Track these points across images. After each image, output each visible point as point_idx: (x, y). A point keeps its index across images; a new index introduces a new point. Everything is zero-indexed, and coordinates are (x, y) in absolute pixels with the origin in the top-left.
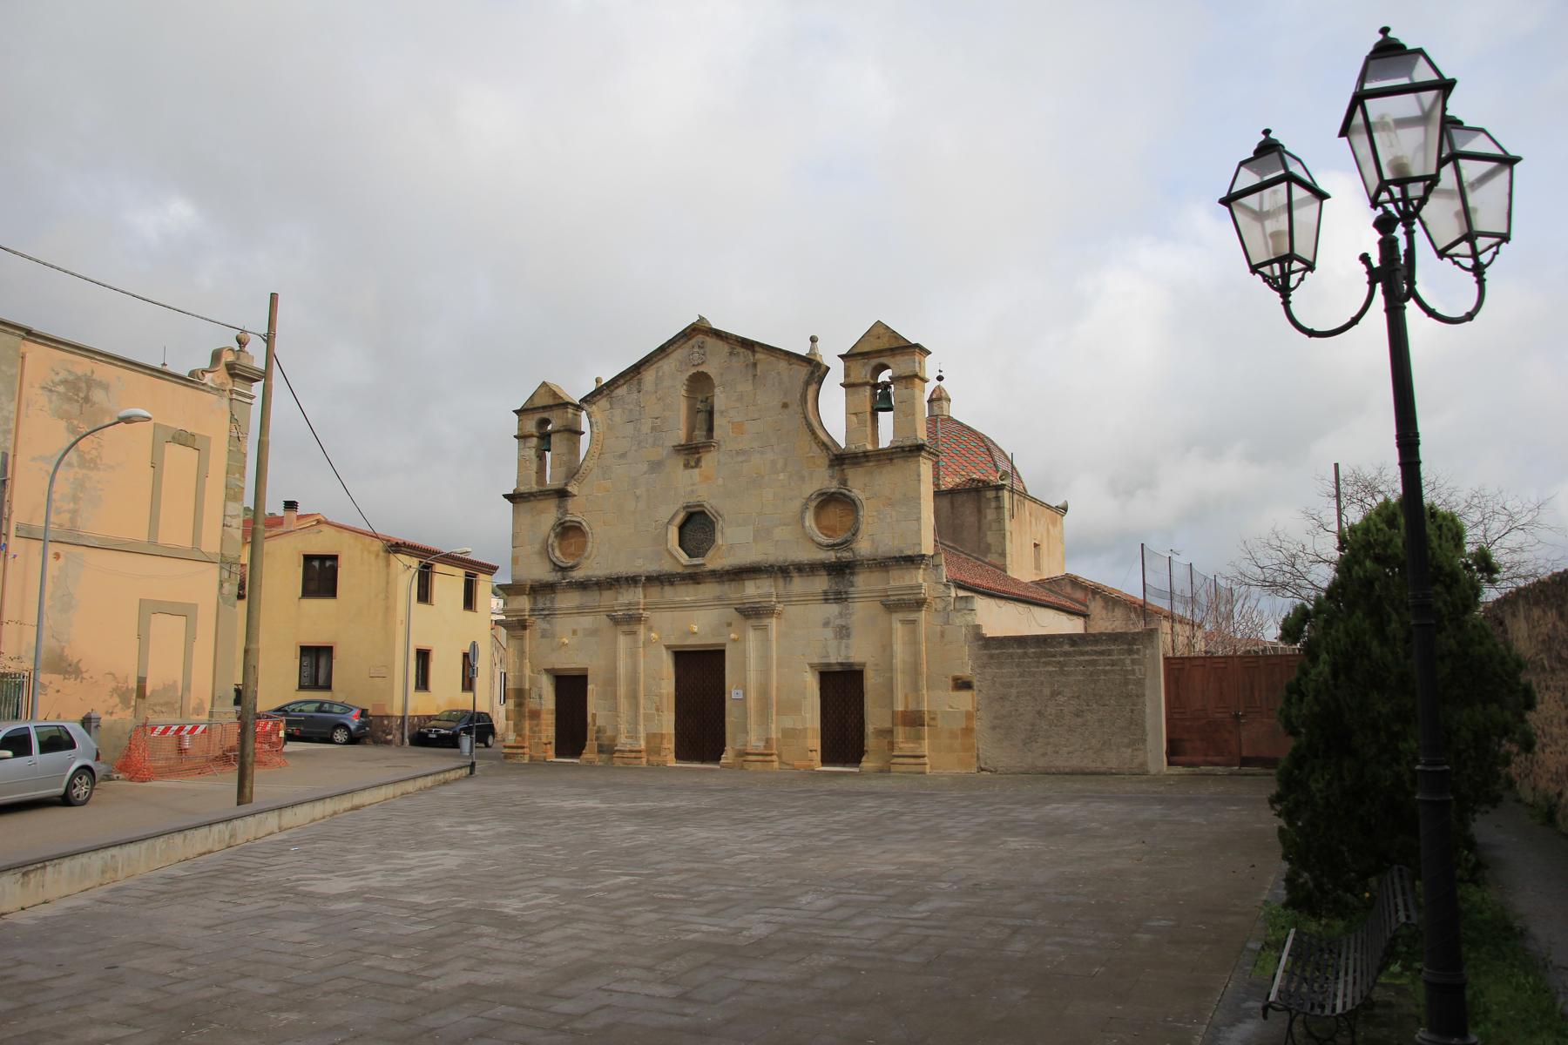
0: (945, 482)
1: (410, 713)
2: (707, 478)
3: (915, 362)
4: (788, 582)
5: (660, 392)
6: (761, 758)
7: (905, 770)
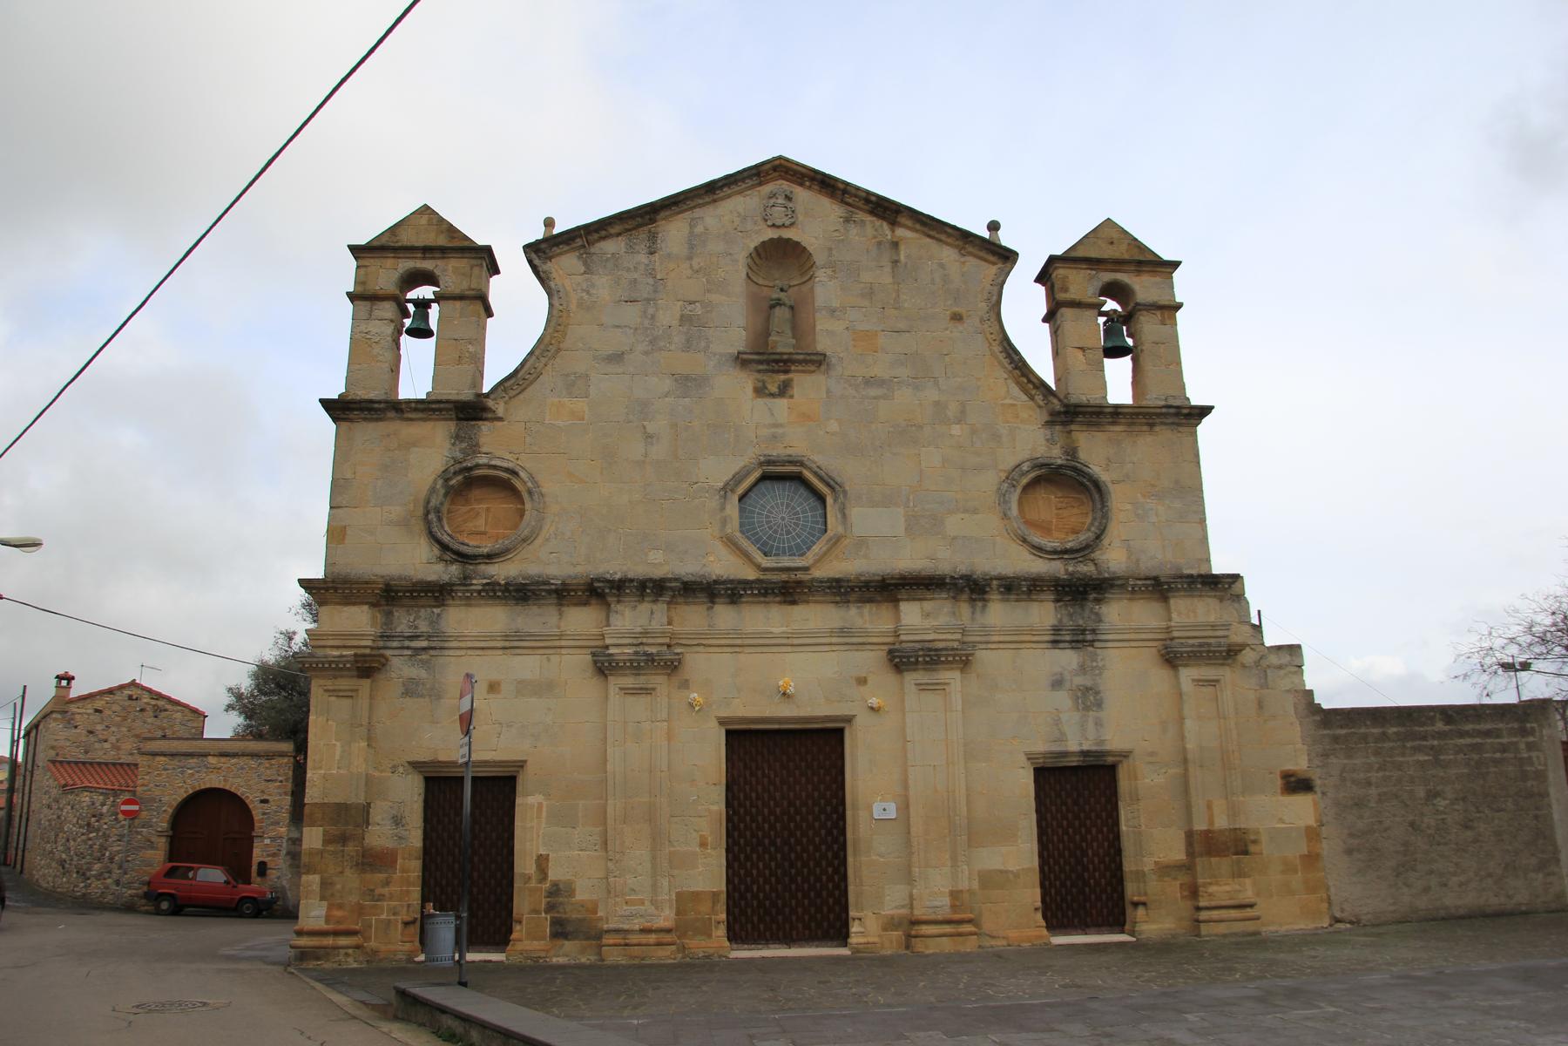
6: (947, 929)
7: (1226, 932)
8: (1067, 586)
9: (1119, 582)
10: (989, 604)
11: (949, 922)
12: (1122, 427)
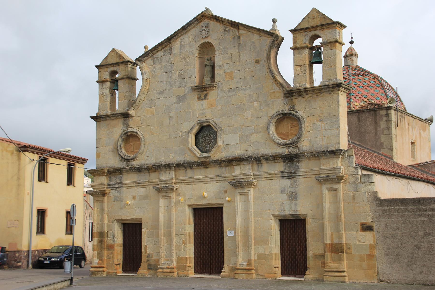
0: (354, 106)
1: (33, 248)
2: (212, 105)
3: (336, 33)
4: (260, 167)
5: (182, 55)
6: (245, 272)
7: (333, 280)
8: (285, 157)
9: (302, 155)
10: (263, 165)
11: (246, 270)
12: (310, 95)
